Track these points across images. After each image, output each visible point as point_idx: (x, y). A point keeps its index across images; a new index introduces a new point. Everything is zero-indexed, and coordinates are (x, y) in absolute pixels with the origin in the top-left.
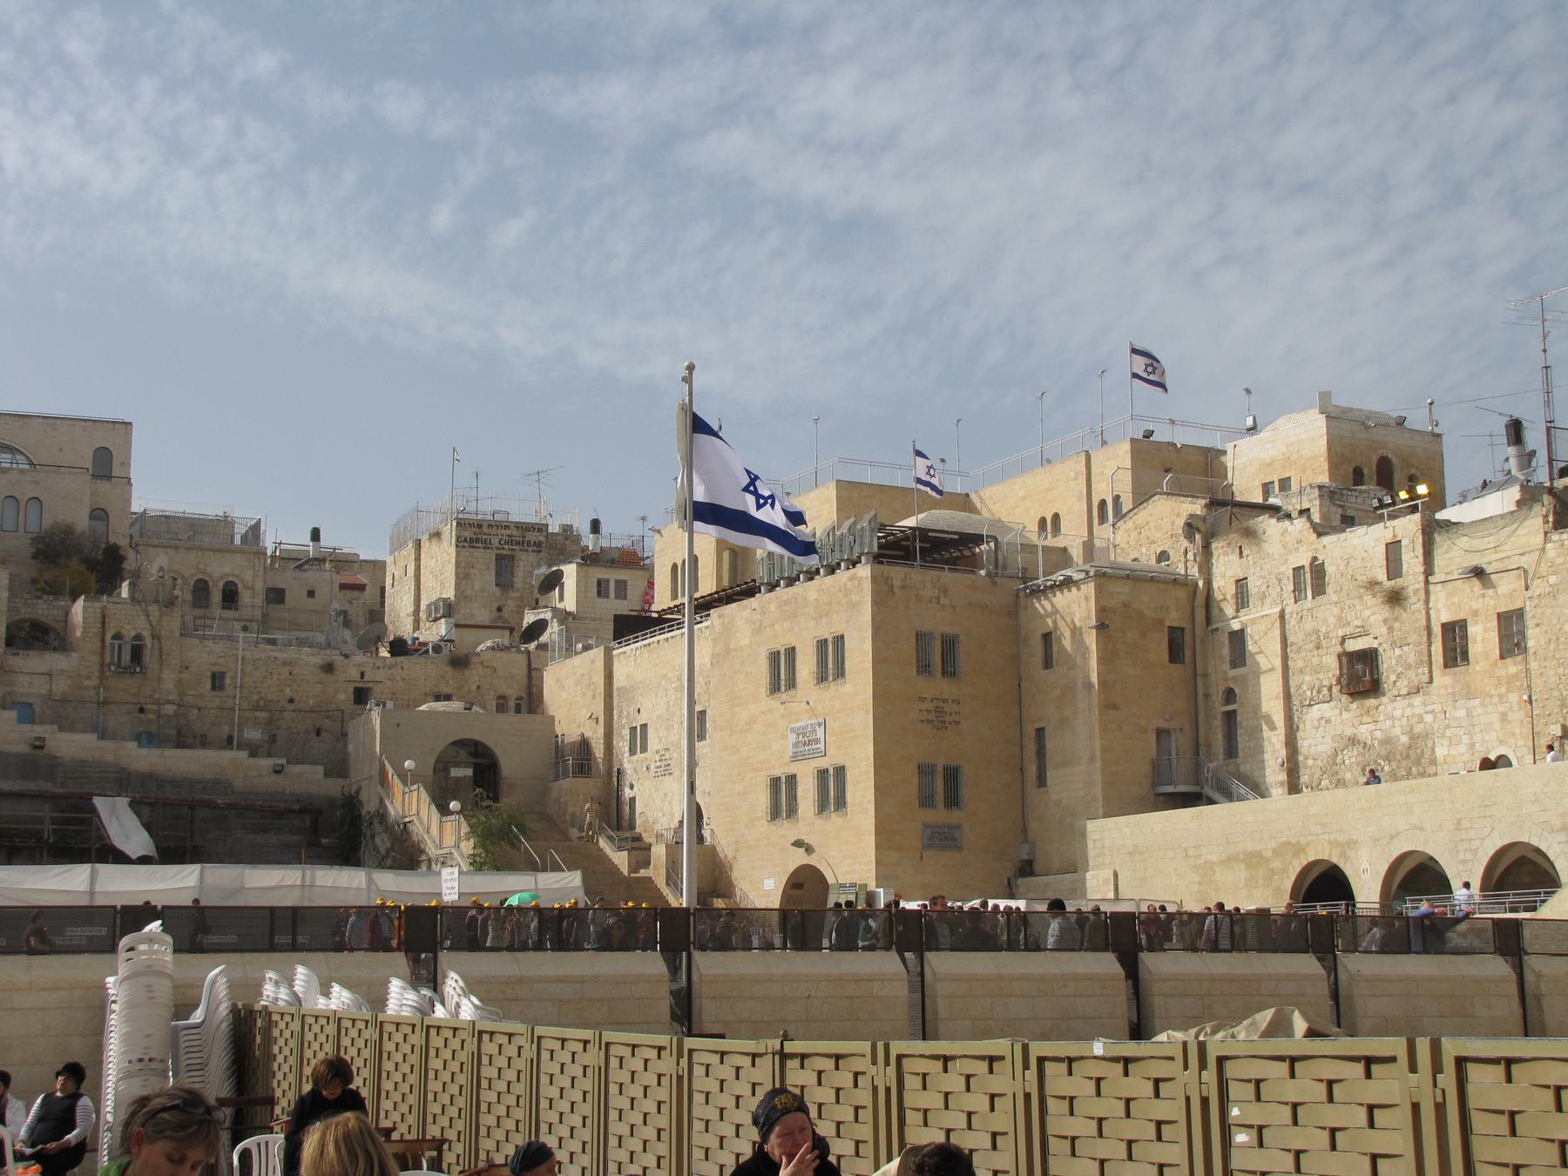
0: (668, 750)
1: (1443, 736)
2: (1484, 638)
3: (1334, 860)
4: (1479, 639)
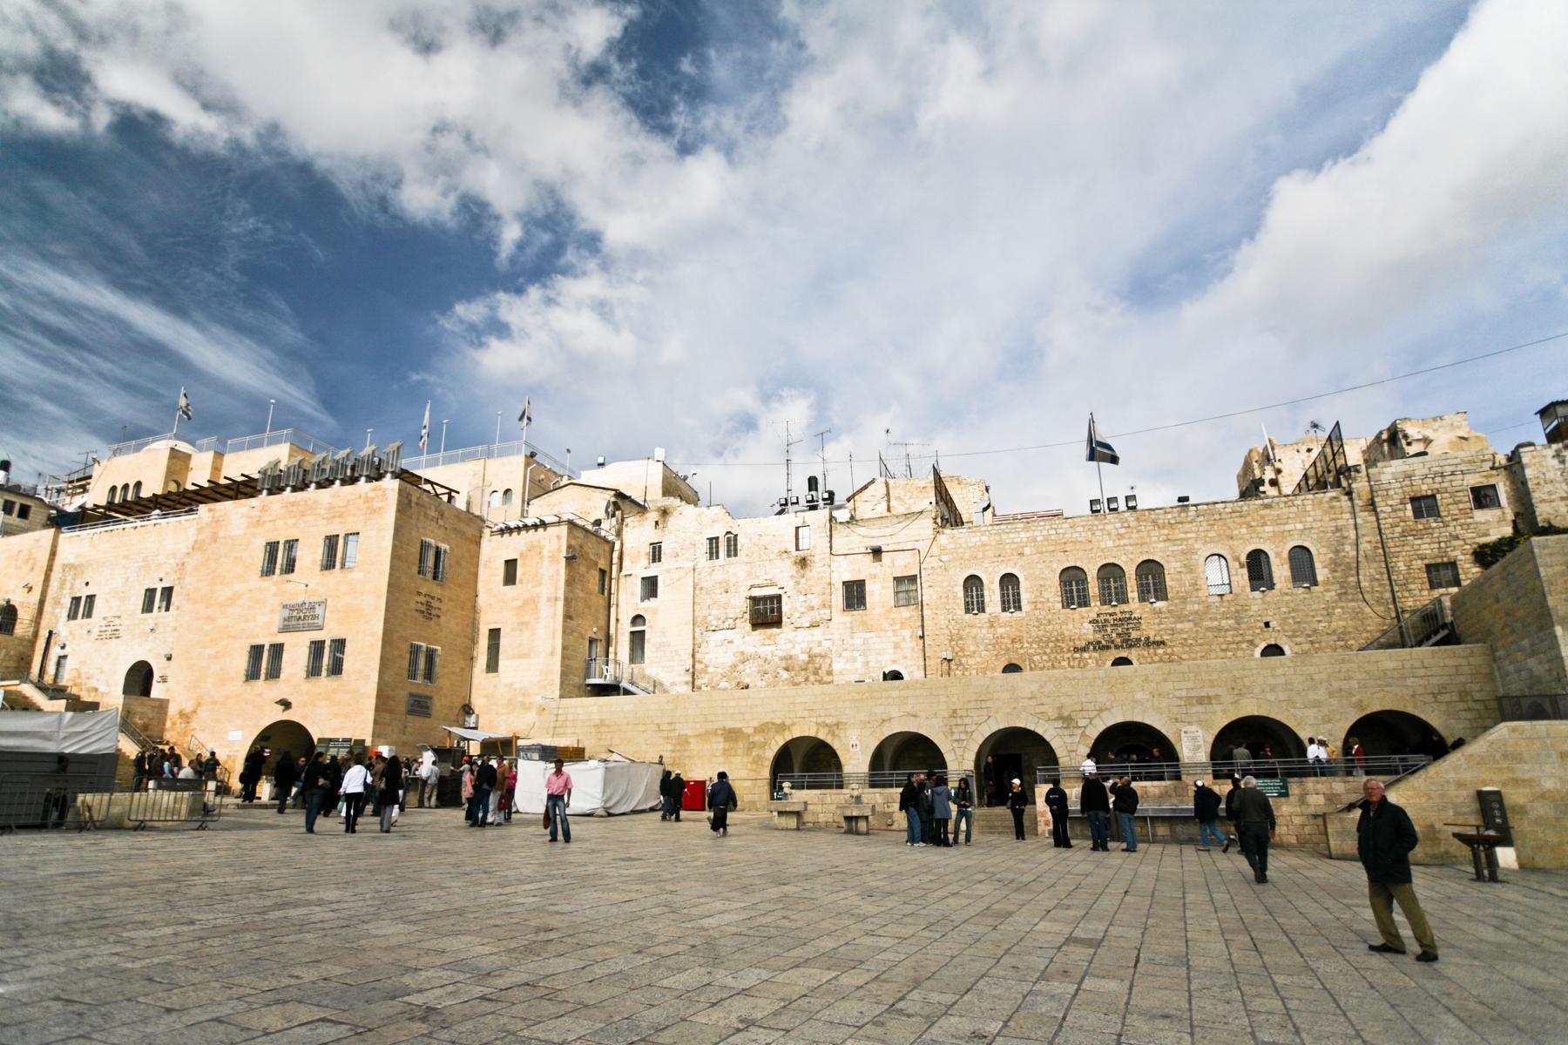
0: (119, 617)
1: (840, 656)
2: (879, 592)
3: (821, 736)
4: (876, 593)
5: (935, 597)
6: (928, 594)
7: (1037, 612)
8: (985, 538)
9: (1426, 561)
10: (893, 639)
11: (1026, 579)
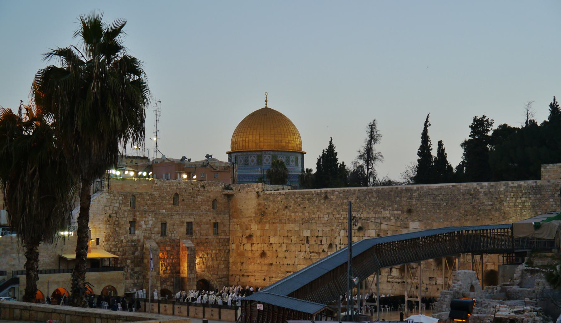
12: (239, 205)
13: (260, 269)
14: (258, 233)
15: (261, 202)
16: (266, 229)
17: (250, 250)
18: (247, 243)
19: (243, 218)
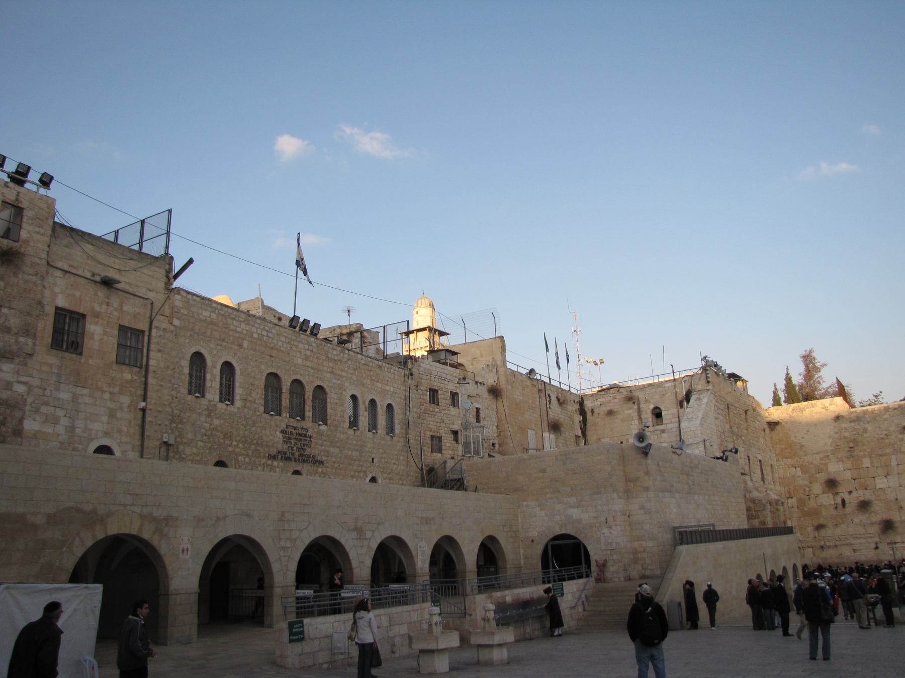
1: (37, 411)
3: (146, 536)
4: (97, 337)
5: (162, 365)
6: (155, 360)
7: (246, 410)
8: (214, 316)
9: (431, 433)
10: (109, 404)
11: (242, 374)
12: (795, 437)
13: (862, 530)
14: (848, 475)
15: (844, 425)
16: (864, 466)
17: (833, 503)
18: (823, 493)
19: (806, 455)
